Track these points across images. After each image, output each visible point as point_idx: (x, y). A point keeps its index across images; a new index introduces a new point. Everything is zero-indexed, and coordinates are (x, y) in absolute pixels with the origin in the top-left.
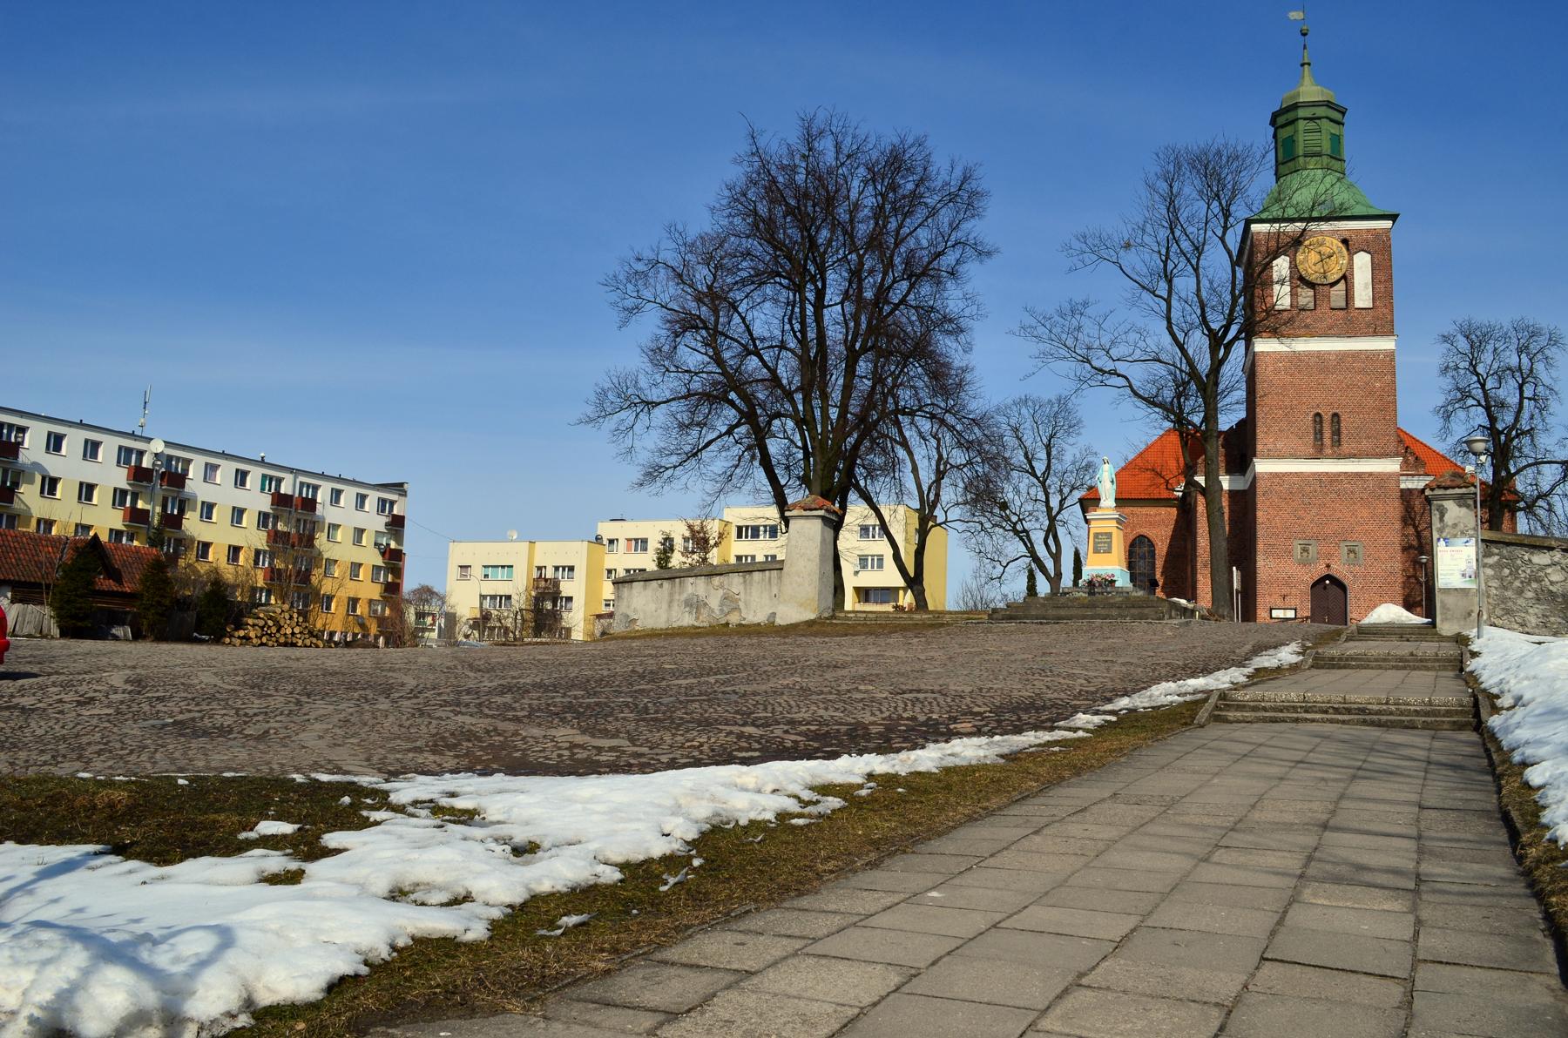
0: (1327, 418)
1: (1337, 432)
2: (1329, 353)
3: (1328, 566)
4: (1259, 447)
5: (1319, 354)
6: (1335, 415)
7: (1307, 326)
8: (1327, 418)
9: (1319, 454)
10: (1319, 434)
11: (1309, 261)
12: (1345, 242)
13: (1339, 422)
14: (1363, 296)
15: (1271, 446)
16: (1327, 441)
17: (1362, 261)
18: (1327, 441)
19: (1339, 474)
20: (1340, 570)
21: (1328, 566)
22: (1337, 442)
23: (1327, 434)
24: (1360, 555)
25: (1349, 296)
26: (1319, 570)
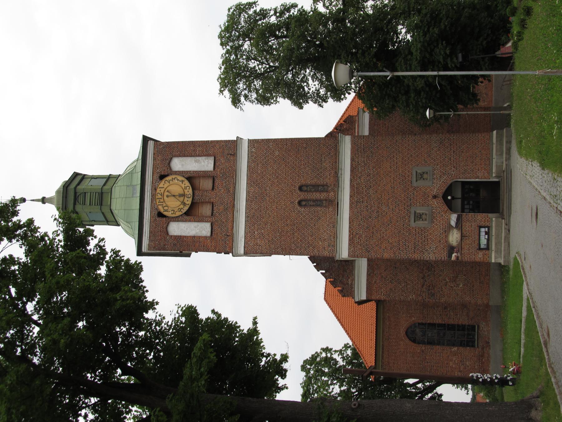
0: (303, 195)
1: (316, 188)
2: (248, 193)
3: (435, 197)
4: (326, 254)
5: (249, 201)
6: (300, 189)
7: (226, 209)
8: (303, 195)
9: (334, 204)
10: (318, 203)
11: (173, 206)
12: (162, 177)
13: (307, 186)
14: (205, 164)
15: (326, 244)
16: (323, 196)
17: (178, 164)
18: (323, 196)
19: (352, 186)
20: (437, 186)
21: (435, 197)
22: (323, 188)
23: (316, 196)
24: (425, 169)
25: (204, 175)
26: (438, 205)
